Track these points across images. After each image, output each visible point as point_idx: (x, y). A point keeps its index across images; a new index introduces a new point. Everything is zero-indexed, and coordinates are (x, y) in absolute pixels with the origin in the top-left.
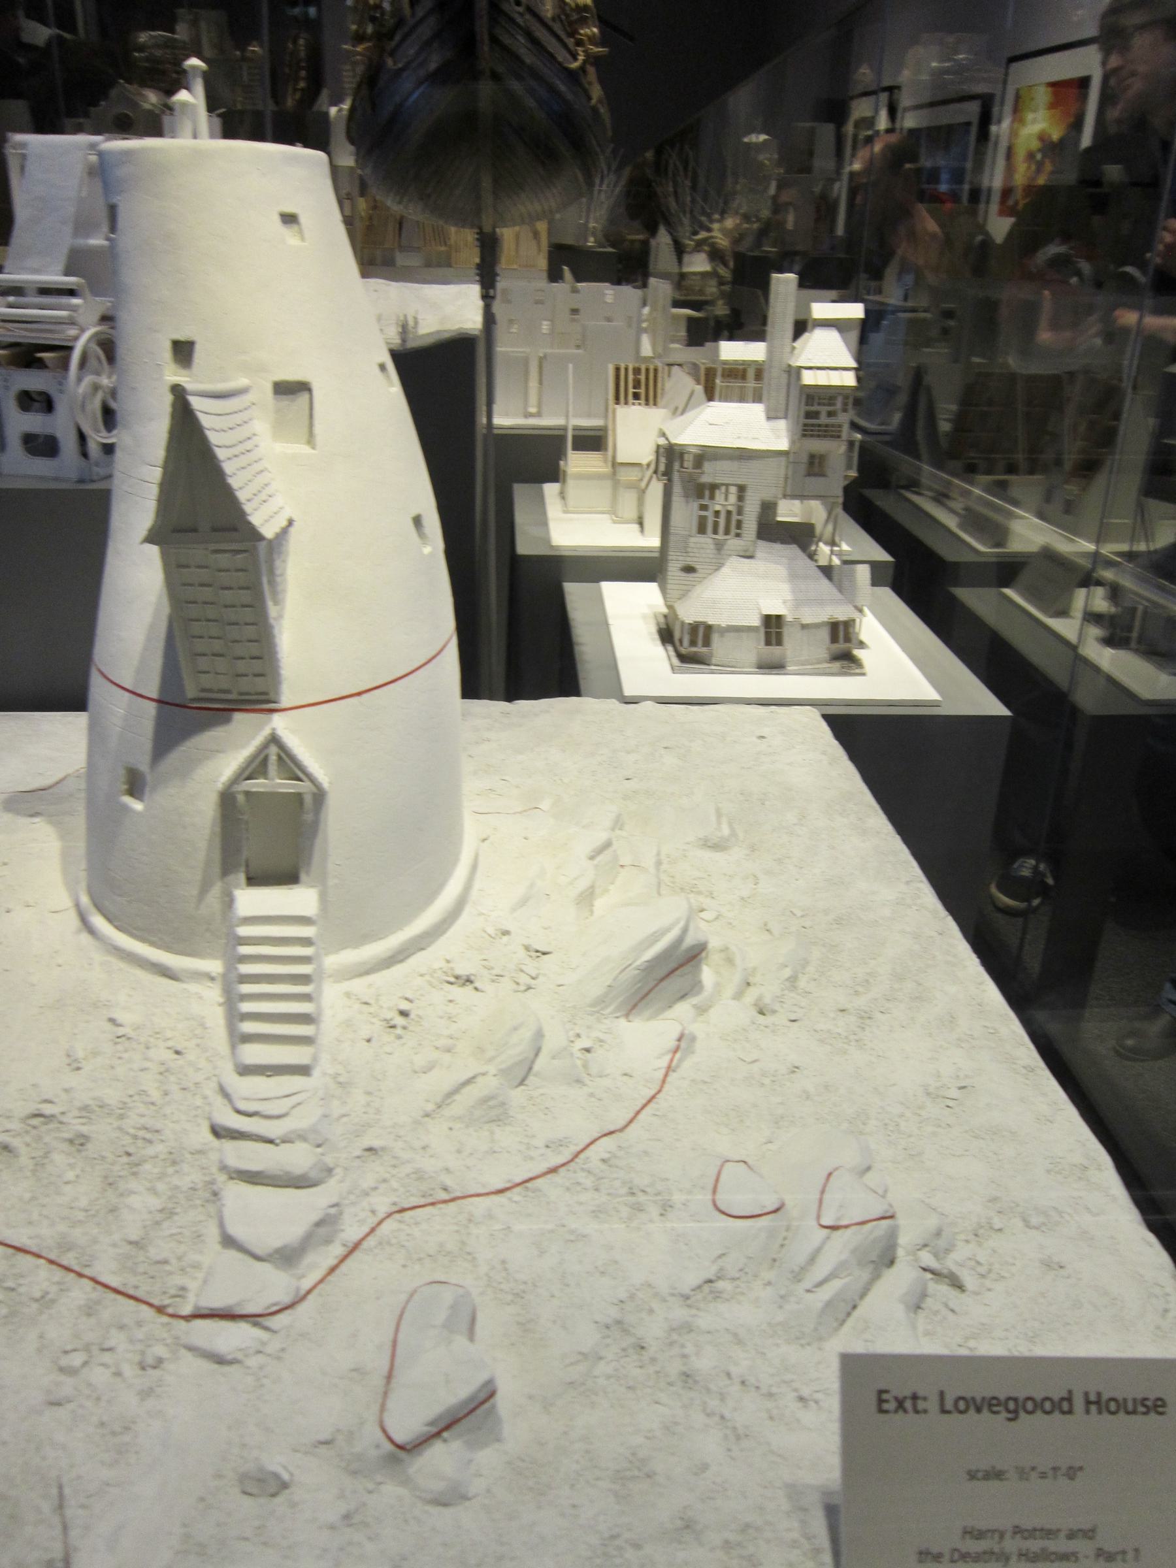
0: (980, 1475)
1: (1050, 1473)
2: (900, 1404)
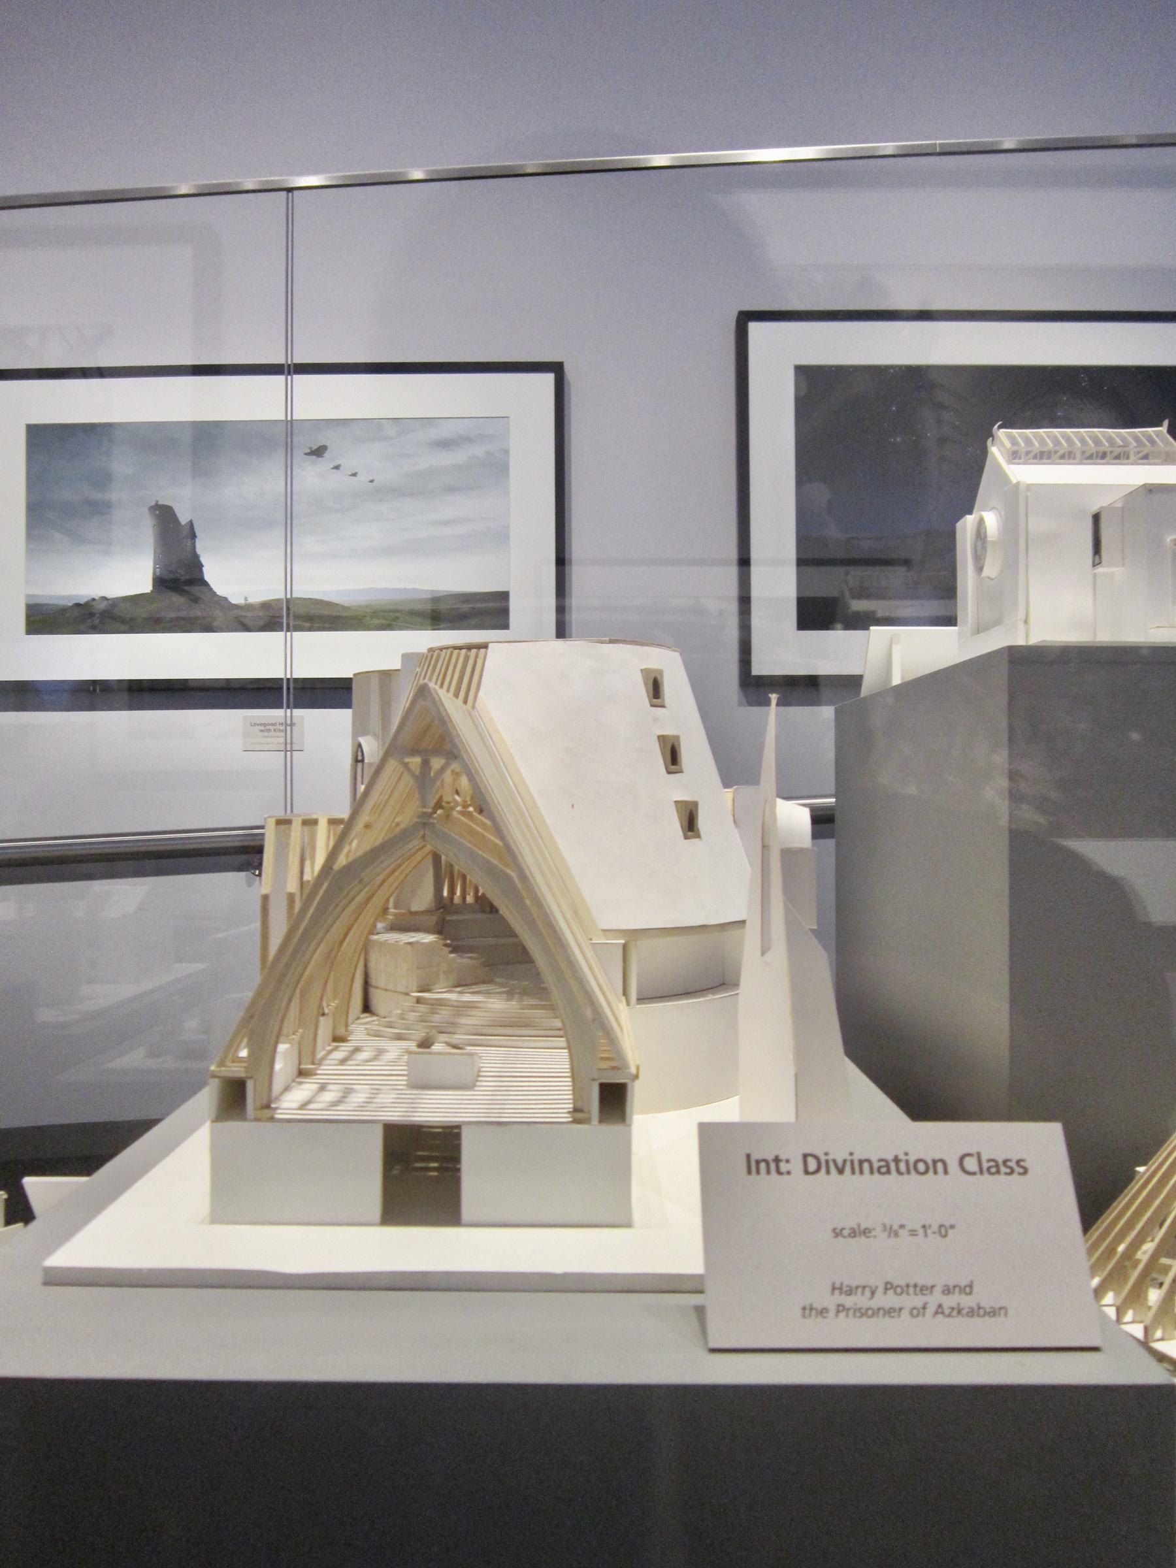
0: (846, 1232)
1: (921, 1231)
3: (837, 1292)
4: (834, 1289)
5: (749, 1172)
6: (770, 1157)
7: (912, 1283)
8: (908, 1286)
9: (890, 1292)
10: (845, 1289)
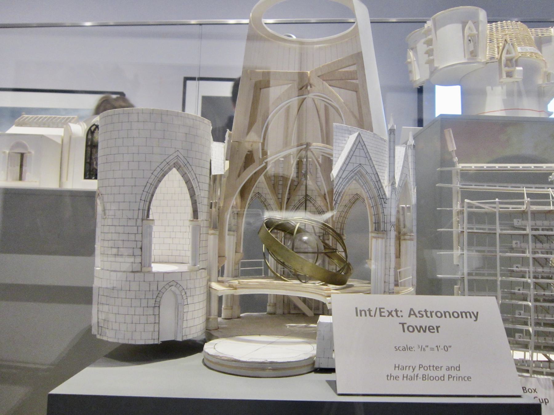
2: (390, 313)
3: (397, 369)
4: (395, 367)
5: (357, 315)
6: (366, 309)
7: (432, 365)
8: (430, 366)
9: (422, 369)
10: (400, 367)
